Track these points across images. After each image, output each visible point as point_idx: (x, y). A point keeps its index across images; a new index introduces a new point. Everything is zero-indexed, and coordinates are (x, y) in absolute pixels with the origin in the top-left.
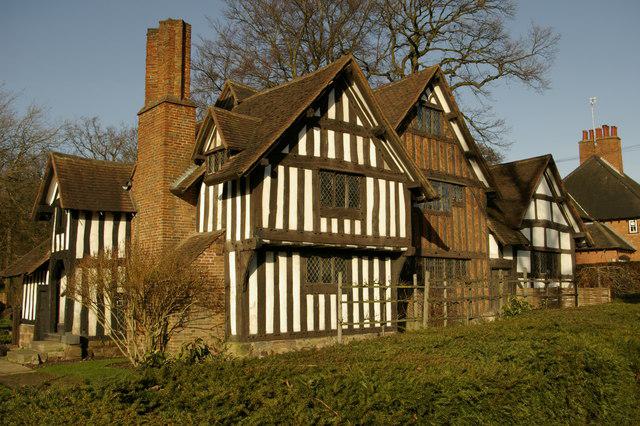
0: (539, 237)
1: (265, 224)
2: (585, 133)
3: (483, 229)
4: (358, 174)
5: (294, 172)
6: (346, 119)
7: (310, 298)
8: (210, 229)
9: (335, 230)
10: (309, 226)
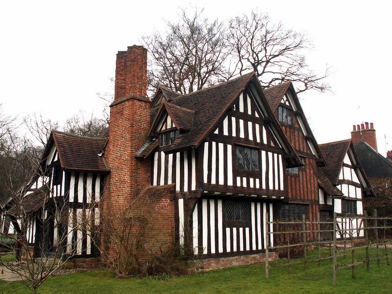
0: (345, 189)
1: (205, 181)
2: (354, 126)
3: (316, 185)
4: (258, 147)
5: (221, 146)
6: (250, 112)
7: (228, 230)
8: (162, 183)
9: (245, 185)
10: (230, 183)
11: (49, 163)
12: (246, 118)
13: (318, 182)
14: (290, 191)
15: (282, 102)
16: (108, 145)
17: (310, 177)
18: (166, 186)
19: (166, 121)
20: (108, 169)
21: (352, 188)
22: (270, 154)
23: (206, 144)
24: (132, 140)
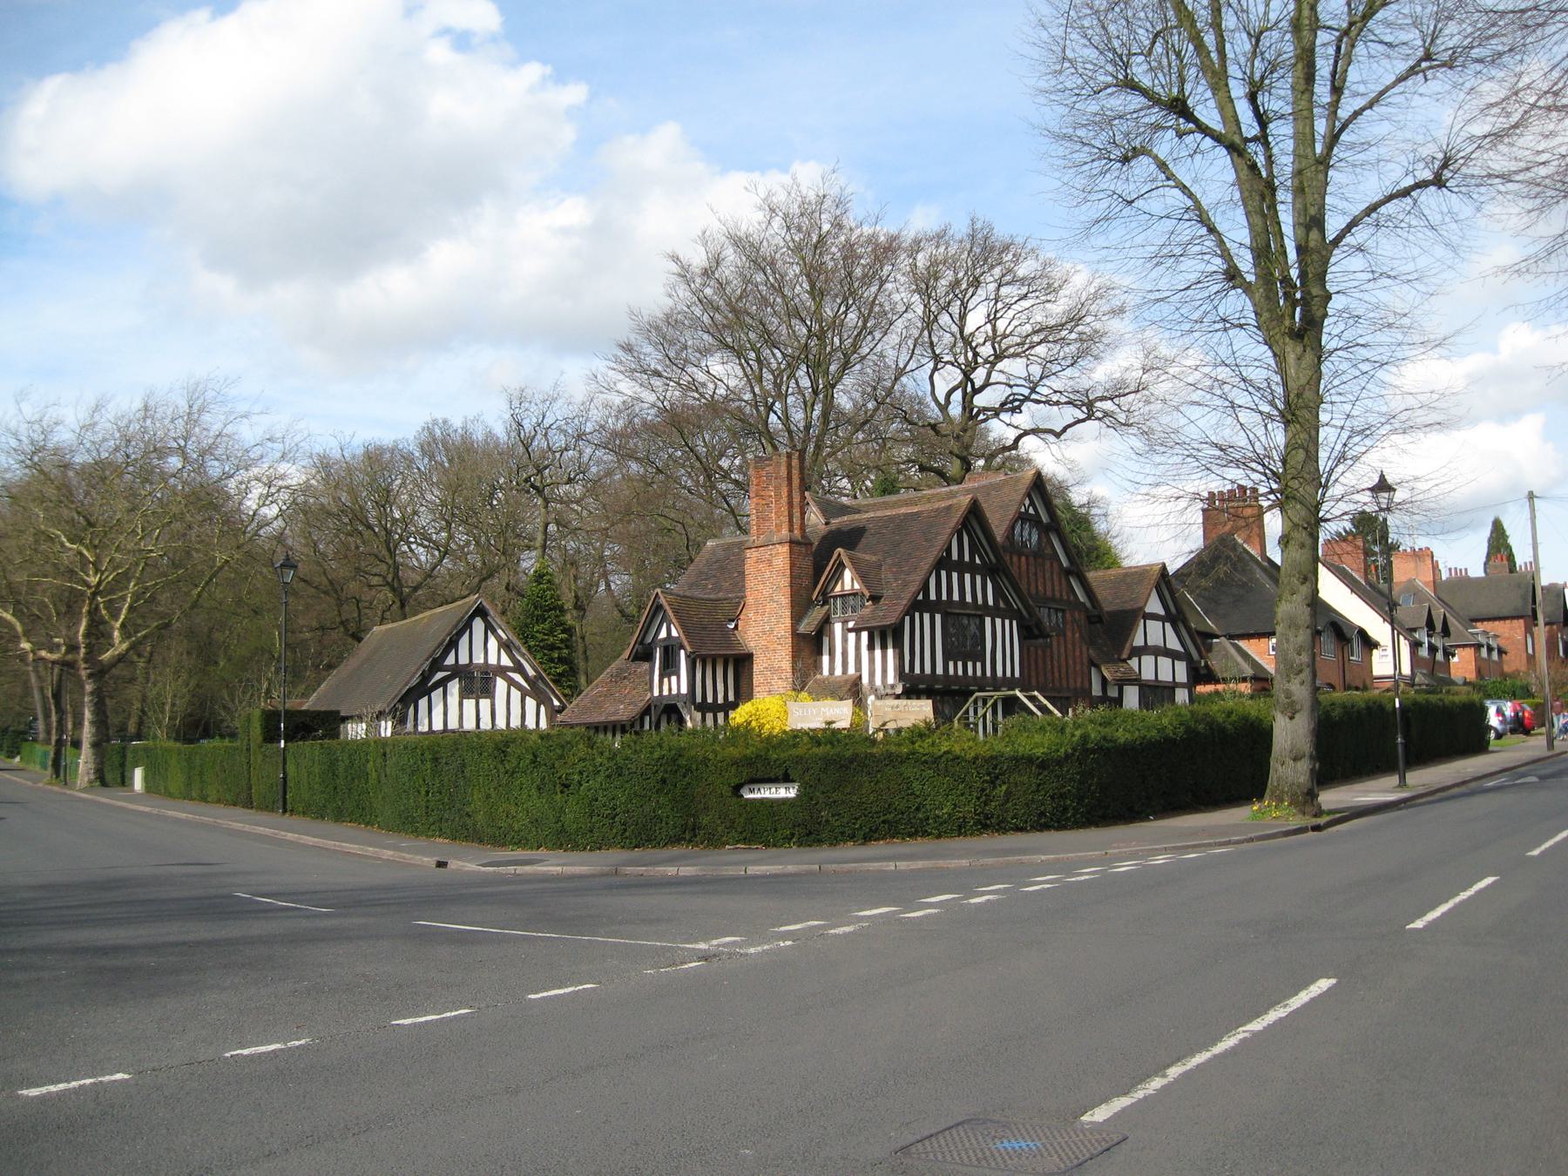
1: (907, 669)
3: (1085, 661)
5: (927, 617)
6: (967, 558)
8: (838, 671)
9: (960, 673)
10: (939, 671)
11: (649, 639)
12: (961, 567)
13: (1089, 655)
14: (1033, 673)
15: (1023, 510)
17: (1074, 644)
18: (845, 677)
21: (1165, 663)
22: (998, 621)
23: (907, 619)
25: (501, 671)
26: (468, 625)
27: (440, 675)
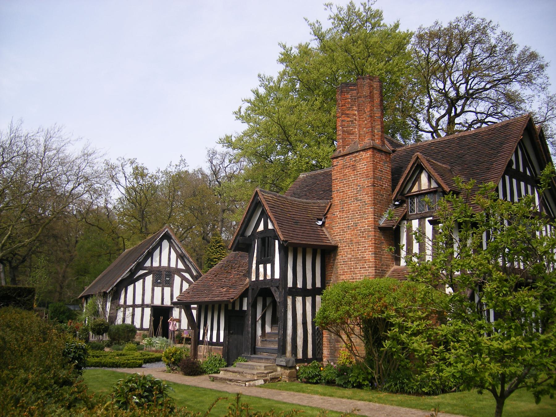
6: (521, 170)
11: (249, 233)
16: (330, 210)
19: (418, 178)
20: (333, 243)
24: (375, 204)
25: (178, 271)
26: (159, 244)
27: (141, 272)
